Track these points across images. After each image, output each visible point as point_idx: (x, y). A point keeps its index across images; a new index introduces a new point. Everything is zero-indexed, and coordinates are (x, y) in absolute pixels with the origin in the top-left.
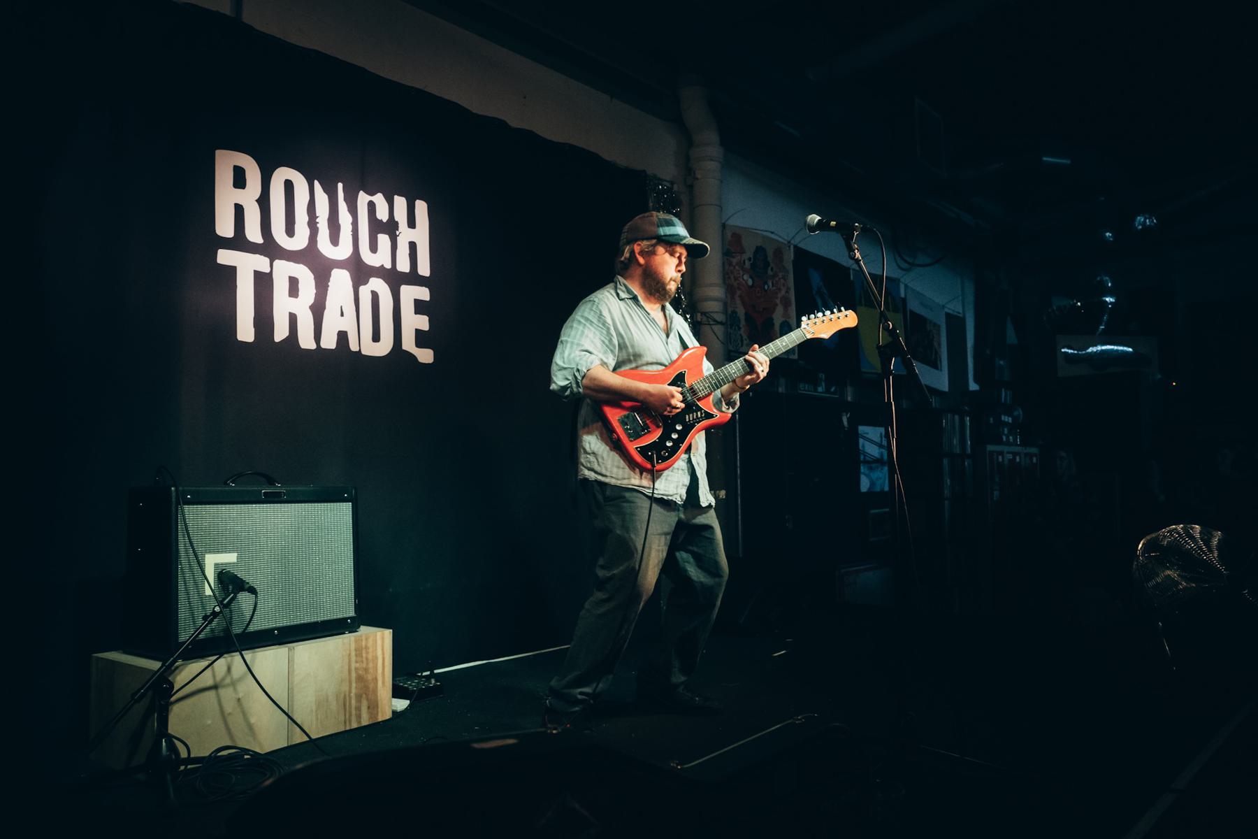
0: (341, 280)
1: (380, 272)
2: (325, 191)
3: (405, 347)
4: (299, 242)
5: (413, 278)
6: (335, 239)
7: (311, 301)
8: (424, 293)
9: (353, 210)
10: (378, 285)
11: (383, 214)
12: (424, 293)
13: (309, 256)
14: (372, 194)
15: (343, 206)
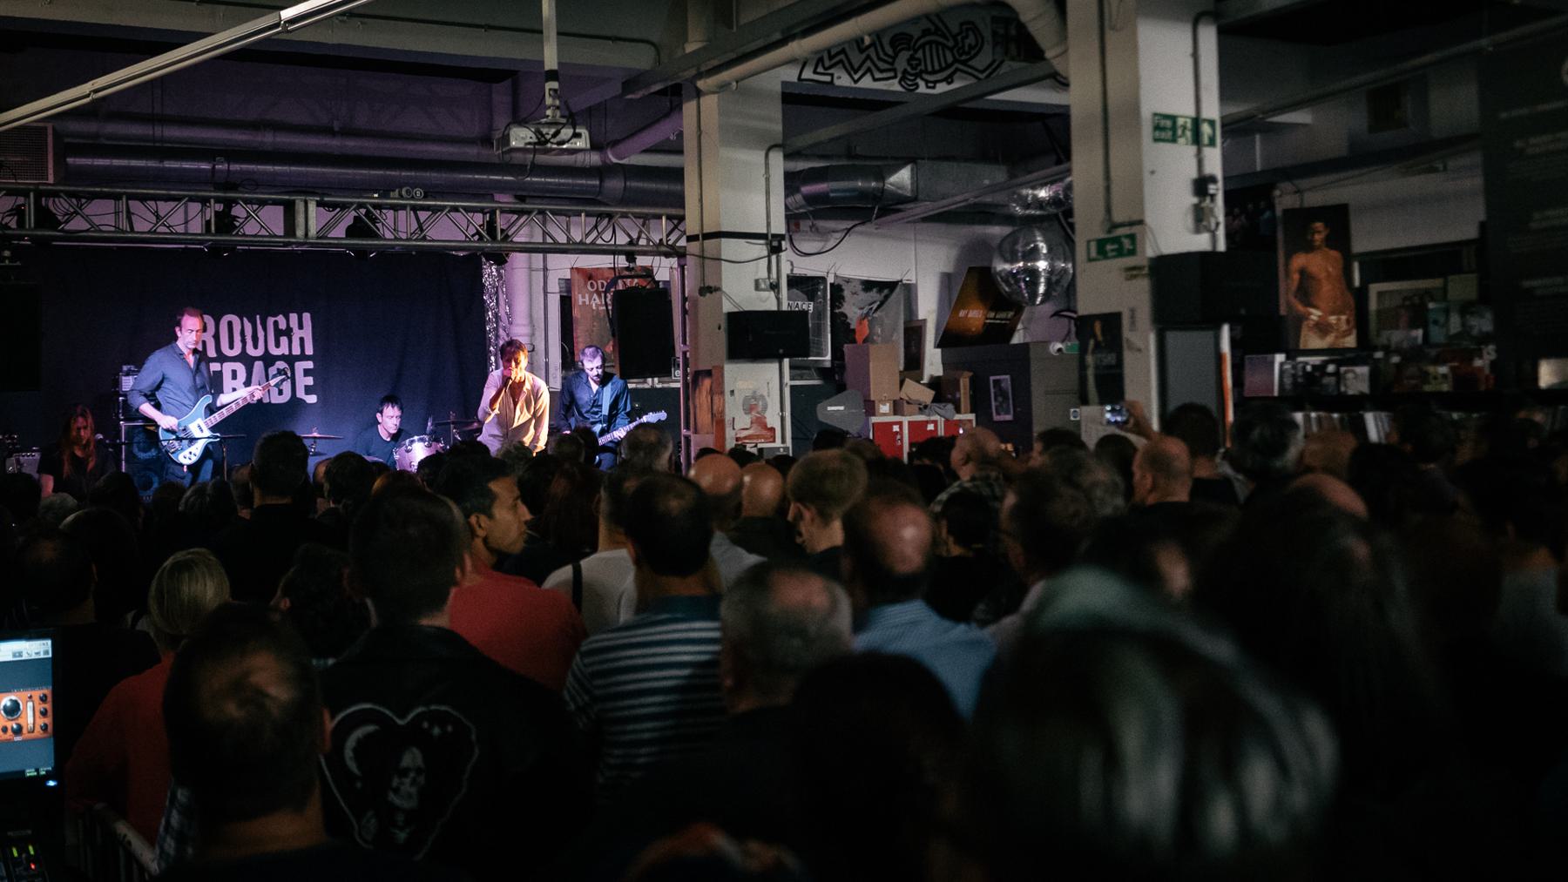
0: (259, 365)
1: (282, 358)
2: (249, 321)
3: (298, 396)
4: (236, 351)
5: (303, 357)
6: (256, 347)
7: (244, 380)
8: (310, 365)
9: (265, 329)
10: (281, 365)
11: (283, 326)
12: (310, 365)
13: (244, 358)
14: (276, 316)
15: (259, 327)
